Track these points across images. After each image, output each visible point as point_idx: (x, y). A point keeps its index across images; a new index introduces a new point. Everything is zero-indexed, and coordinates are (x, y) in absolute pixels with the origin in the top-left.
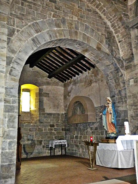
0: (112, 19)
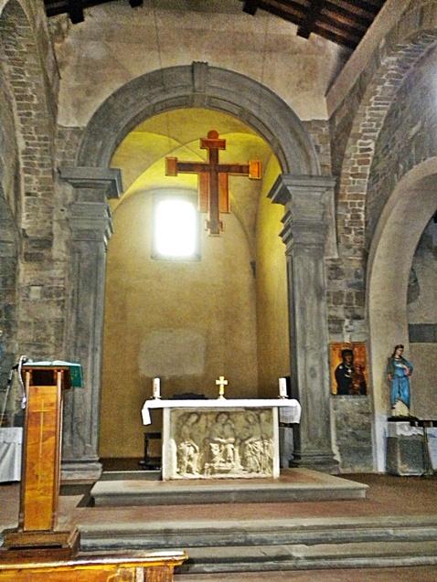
0: (34, 139)
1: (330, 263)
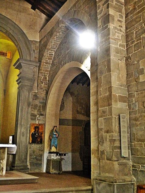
1: (34, 93)
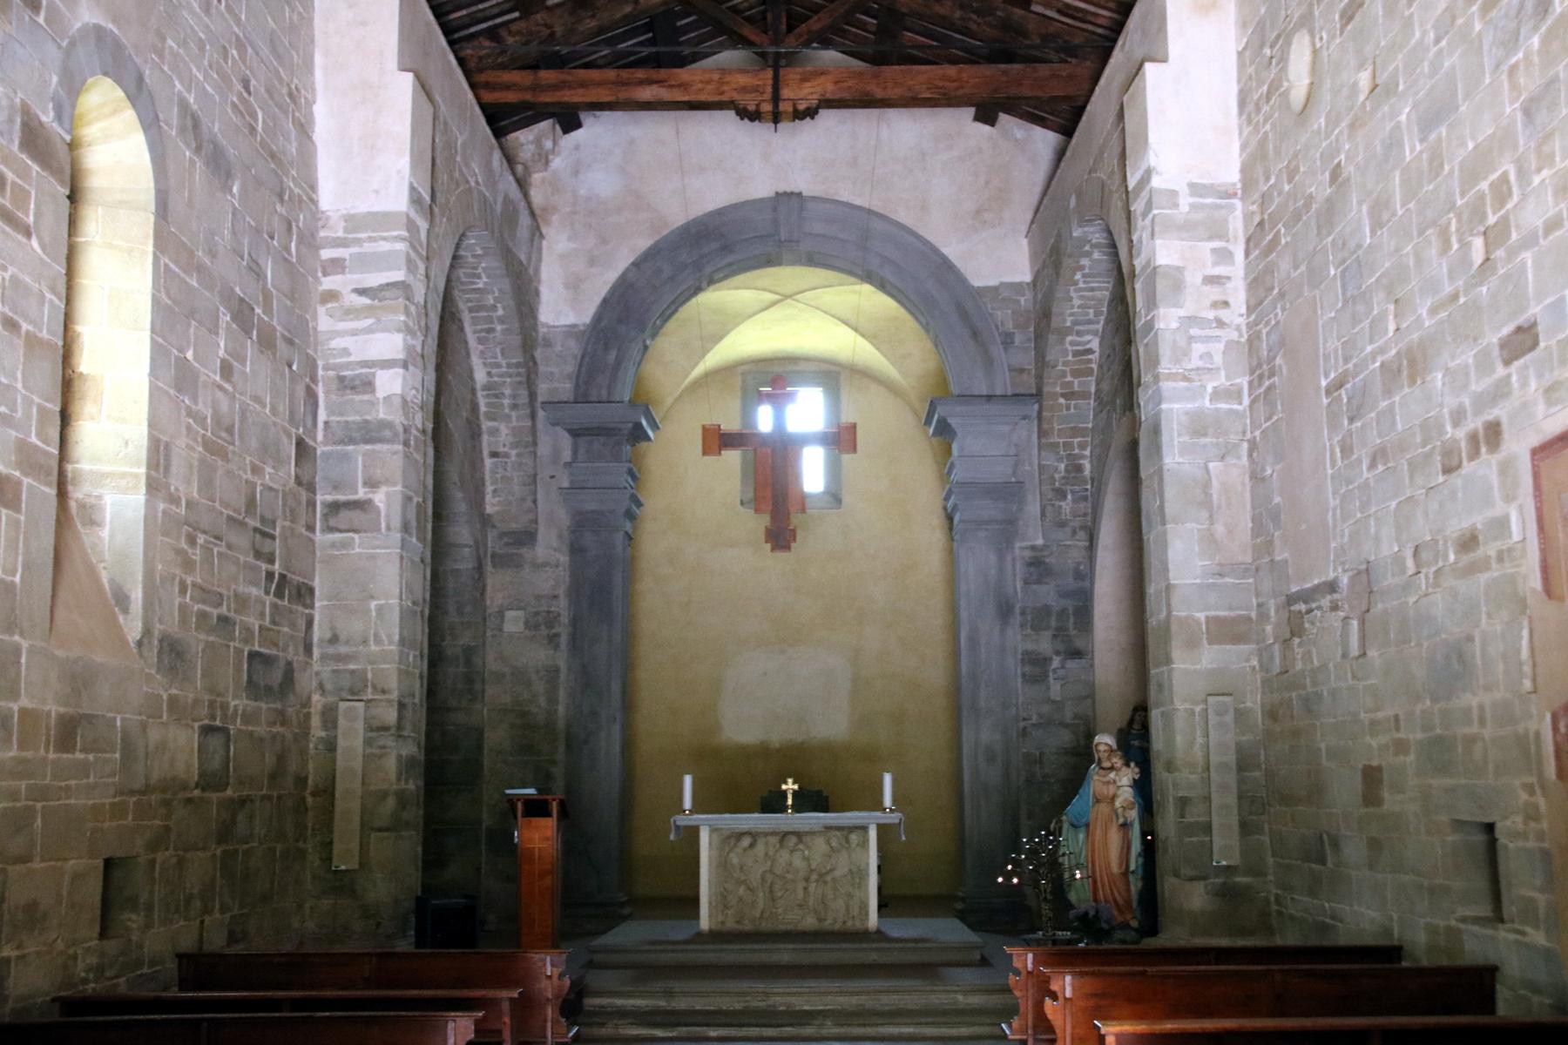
0: (498, 366)
1: (1028, 554)
